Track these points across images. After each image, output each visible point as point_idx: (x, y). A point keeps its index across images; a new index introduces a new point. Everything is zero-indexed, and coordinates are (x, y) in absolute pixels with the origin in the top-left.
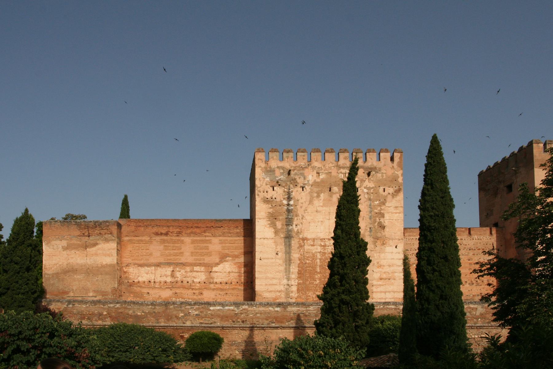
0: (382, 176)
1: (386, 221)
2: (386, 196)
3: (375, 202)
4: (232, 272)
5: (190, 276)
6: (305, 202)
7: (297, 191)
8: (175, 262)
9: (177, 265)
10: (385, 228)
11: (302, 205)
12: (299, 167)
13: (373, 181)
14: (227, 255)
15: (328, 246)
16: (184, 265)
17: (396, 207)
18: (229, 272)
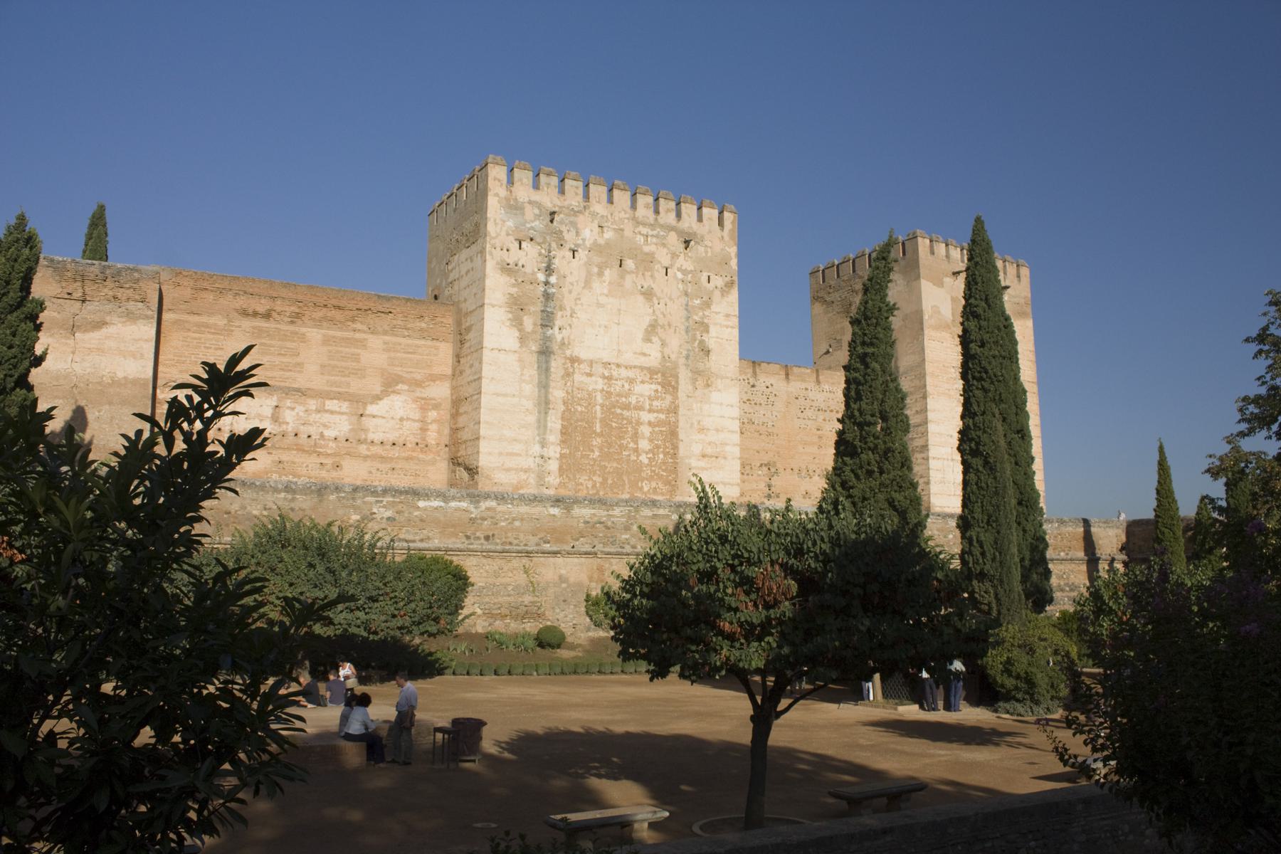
0: (706, 252)
1: (711, 343)
2: (712, 291)
3: (695, 301)
4: (408, 419)
5: (315, 423)
6: (577, 282)
7: (564, 257)
8: (283, 384)
9: (287, 394)
10: (711, 353)
11: (571, 287)
12: (568, 208)
13: (691, 258)
14: (398, 379)
15: (617, 380)
16: (303, 393)
17: (728, 316)
18: (401, 419)
